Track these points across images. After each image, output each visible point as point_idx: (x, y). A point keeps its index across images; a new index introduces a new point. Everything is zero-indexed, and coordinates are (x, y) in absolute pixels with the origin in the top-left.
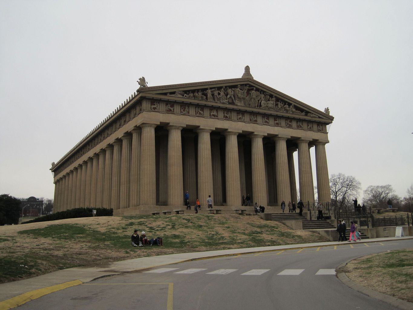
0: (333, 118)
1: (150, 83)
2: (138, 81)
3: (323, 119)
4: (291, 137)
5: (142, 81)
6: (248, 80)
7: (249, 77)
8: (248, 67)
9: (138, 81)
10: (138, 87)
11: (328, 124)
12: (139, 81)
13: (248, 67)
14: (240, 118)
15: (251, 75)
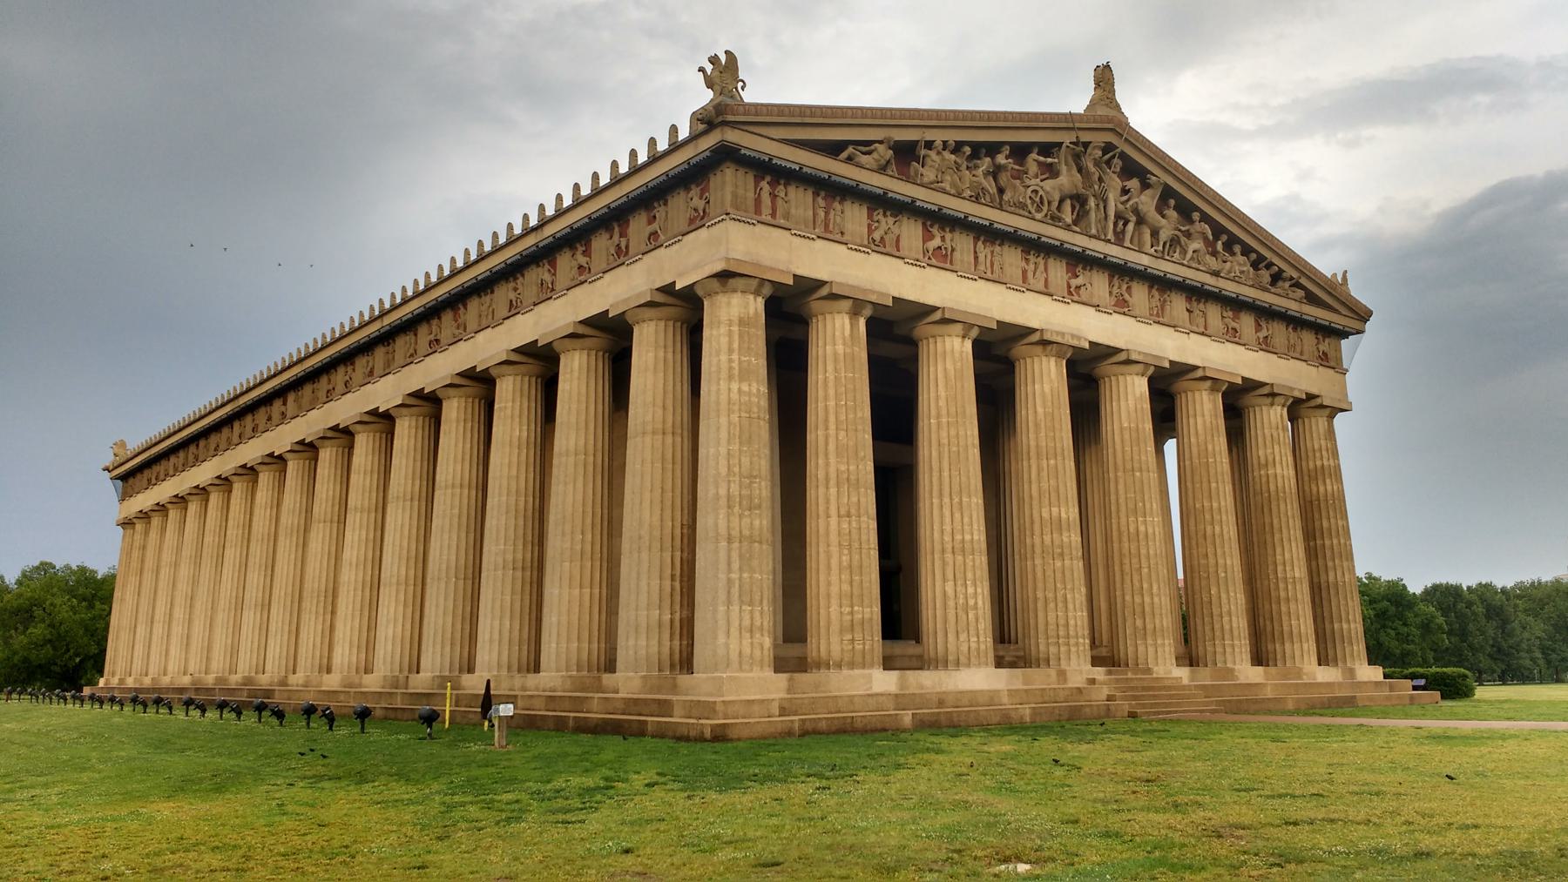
0: (1370, 314)
1: (756, 91)
2: (701, 70)
3: (1340, 313)
4: (1243, 378)
5: (723, 72)
6: (1110, 126)
7: (1112, 113)
8: (1107, 67)
9: (701, 70)
10: (704, 97)
11: (1344, 334)
12: (709, 68)
13: (1107, 67)
14: (1078, 288)
15: (1118, 107)
